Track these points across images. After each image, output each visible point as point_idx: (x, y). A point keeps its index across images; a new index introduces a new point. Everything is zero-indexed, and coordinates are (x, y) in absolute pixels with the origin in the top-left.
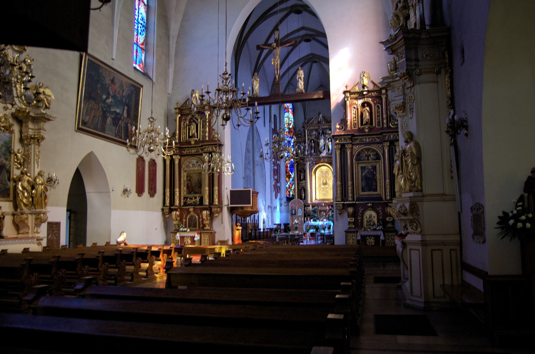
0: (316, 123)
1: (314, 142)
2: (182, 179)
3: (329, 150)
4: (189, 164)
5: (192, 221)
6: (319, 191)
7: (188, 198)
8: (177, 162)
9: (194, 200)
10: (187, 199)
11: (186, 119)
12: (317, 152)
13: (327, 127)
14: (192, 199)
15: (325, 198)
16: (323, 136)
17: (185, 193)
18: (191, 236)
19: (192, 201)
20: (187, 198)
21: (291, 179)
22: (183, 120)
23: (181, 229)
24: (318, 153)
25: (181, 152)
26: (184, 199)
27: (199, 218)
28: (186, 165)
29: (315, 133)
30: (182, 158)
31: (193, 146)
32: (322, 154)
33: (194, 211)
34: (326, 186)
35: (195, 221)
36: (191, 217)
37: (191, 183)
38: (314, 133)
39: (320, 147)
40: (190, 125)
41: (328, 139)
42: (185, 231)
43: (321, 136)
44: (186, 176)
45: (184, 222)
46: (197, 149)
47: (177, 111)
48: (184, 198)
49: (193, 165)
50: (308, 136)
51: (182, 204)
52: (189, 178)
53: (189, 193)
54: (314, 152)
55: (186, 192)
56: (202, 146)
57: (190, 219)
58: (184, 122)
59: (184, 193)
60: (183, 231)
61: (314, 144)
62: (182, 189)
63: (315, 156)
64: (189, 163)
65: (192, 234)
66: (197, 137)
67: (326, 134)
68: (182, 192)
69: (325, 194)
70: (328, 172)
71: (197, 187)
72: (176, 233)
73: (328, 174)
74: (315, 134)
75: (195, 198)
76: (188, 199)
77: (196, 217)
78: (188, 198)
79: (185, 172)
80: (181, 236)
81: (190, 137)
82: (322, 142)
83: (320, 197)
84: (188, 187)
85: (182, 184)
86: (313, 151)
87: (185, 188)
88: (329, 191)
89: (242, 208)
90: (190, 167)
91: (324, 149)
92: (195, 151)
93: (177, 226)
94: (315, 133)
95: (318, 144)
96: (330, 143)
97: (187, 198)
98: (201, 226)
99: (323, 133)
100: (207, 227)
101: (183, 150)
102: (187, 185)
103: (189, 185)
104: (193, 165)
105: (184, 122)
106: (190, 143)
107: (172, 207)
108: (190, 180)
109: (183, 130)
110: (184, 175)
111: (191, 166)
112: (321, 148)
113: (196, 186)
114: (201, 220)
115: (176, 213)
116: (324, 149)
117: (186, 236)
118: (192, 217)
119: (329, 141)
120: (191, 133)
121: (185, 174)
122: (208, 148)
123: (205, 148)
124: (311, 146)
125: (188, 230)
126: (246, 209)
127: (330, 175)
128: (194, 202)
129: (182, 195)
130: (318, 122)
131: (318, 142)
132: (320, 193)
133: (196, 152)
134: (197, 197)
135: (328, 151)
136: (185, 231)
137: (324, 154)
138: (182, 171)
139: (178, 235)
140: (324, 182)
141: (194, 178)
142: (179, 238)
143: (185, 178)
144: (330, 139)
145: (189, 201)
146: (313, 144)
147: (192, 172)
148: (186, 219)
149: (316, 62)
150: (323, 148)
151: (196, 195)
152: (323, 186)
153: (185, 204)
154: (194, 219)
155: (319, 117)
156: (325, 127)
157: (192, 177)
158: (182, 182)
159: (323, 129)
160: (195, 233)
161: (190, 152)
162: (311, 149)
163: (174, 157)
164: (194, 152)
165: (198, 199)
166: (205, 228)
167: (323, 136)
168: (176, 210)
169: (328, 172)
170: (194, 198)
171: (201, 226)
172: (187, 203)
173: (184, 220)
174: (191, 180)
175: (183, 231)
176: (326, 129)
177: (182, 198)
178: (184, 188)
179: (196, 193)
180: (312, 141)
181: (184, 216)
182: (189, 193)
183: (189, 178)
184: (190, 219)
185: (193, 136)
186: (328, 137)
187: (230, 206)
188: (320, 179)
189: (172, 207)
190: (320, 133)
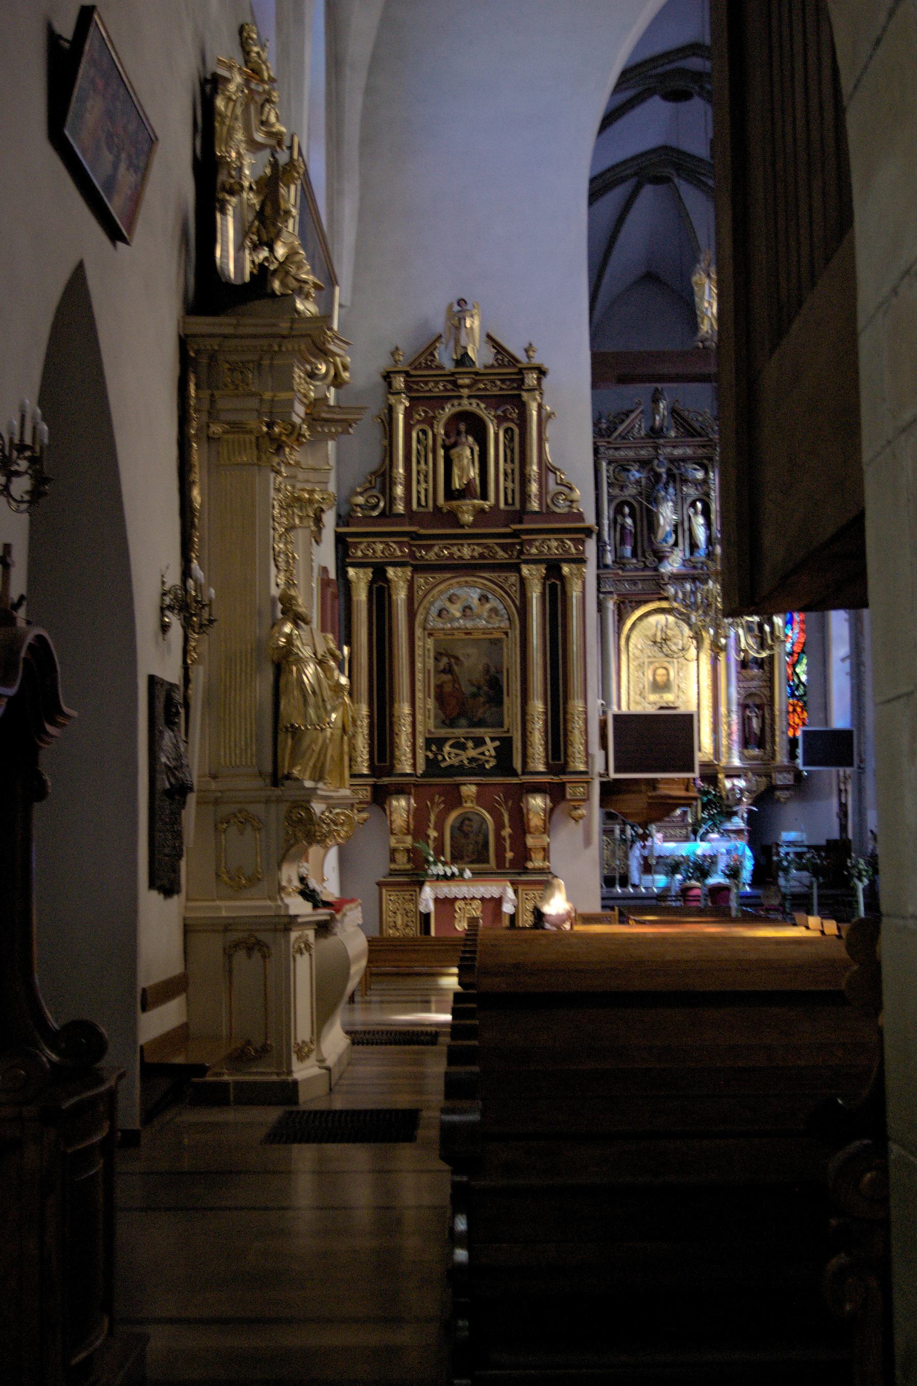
0: (643, 433)
1: (632, 515)
2: (419, 665)
3: (694, 546)
4: (448, 604)
5: (466, 835)
7: (444, 740)
8: (400, 596)
9: (472, 753)
10: (440, 749)
11: (434, 417)
12: (644, 552)
13: (689, 451)
14: (463, 747)
16: (671, 490)
17: (431, 723)
18: (487, 896)
19: (464, 756)
20: (440, 742)
22: (418, 422)
23: (439, 869)
24: (651, 560)
25: (412, 555)
26: (428, 747)
27: (499, 826)
28: (434, 611)
30: (420, 580)
31: (467, 531)
32: (666, 563)
33: (480, 799)
35: (481, 839)
36: (462, 822)
37: (455, 680)
38: (635, 474)
39: (661, 534)
40: (455, 445)
41: (693, 505)
42: (453, 874)
43: (666, 489)
44: (432, 654)
45: (431, 842)
46: (487, 547)
47: (399, 382)
48: (429, 742)
49: (467, 609)
50: (610, 485)
51: (421, 768)
52: (445, 660)
53: (450, 722)
54: (634, 554)
55: (435, 718)
56: (515, 534)
57: (460, 828)
58: (424, 432)
59: (427, 724)
60: (445, 878)
62: (419, 703)
63: (636, 569)
64: (450, 600)
65: (490, 889)
66: (484, 496)
67: (685, 481)
68: (419, 717)
71: (482, 699)
72: (421, 884)
74: (638, 482)
75: (479, 742)
76: (447, 748)
77: (484, 820)
78: (444, 740)
79: (430, 635)
80: (441, 896)
81: (451, 494)
82: (667, 515)
84: (441, 698)
85: (419, 685)
86: (628, 551)
87: (431, 704)
89: (653, 784)
90: (453, 619)
91: (676, 544)
92: (476, 554)
93: (402, 858)
95: (652, 524)
96: (701, 520)
97: (440, 742)
98: (509, 855)
99: (671, 476)
100: (536, 862)
101: (420, 547)
102: (439, 687)
103: (448, 688)
104: (467, 609)
105: (424, 432)
106: (452, 519)
107: (386, 780)
108: (448, 670)
109: (418, 462)
110: (426, 646)
111: (458, 614)
112: (665, 540)
113: (474, 696)
114: (507, 832)
115: (409, 804)
116: (676, 544)
117: (464, 899)
118: (464, 819)
119: (696, 513)
120: (460, 478)
121: (430, 643)
122: (544, 541)
123: (530, 542)
124: (623, 527)
125: (468, 874)
126: (664, 790)
128: (471, 760)
129: (419, 728)
130: (652, 429)
131: (649, 511)
133: (482, 556)
134: (488, 740)
135: (692, 553)
136: (453, 874)
137: (673, 564)
138: (418, 632)
139: (428, 893)
140: (658, 678)
141: (467, 663)
142: (432, 907)
143: (431, 662)
144: (699, 505)
145: (449, 756)
146: (629, 521)
147: (459, 635)
148: (440, 828)
149: (658, 180)
150: (671, 541)
151: (479, 732)
153: (432, 765)
154: (475, 826)
155: (655, 411)
156: (678, 452)
157: (457, 658)
158: (419, 676)
159: (673, 460)
160: (503, 883)
161: (451, 554)
162: (623, 542)
163: (391, 572)
164: (473, 557)
165: (490, 748)
166: (530, 865)
167: (671, 490)
168: (401, 790)
170: (470, 744)
171: (509, 855)
172: (443, 765)
173: (433, 834)
174: (456, 668)
175: (445, 878)
176: (684, 460)
177: (420, 741)
178: (427, 704)
179: (480, 723)
180: (627, 510)
181: (433, 818)
182: (450, 722)
183: (445, 660)
184: (460, 829)
185: (465, 493)
186: (688, 495)
187: (613, 775)
188: (641, 666)
189: (386, 780)
190: (658, 476)
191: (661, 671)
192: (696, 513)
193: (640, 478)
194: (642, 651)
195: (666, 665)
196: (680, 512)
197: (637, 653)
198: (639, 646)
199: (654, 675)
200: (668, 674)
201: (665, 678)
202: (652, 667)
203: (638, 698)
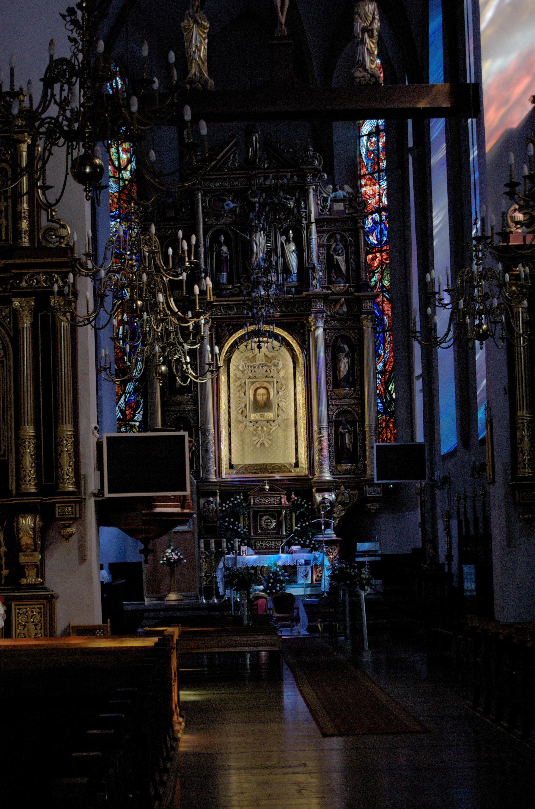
1: (226, 243)
3: (287, 270)
6: (242, 434)
15: (262, 461)
21: (130, 387)
29: (232, 205)
34: (270, 415)
61: (229, 249)
69: (262, 444)
70: (274, 357)
73: (276, 365)
83: (243, 455)
88: (280, 433)
94: (232, 205)
127: (282, 374)
132: (242, 441)
140: (259, 398)
152: (254, 416)
169: (274, 357)
188: (242, 386)
191: (261, 391)
192: (288, 241)
193: (235, 207)
194: (243, 372)
195: (266, 384)
196: (273, 239)
197: (239, 374)
198: (240, 367)
199: (255, 394)
200: (268, 393)
201: (265, 397)
202: (252, 388)
203: (240, 417)
